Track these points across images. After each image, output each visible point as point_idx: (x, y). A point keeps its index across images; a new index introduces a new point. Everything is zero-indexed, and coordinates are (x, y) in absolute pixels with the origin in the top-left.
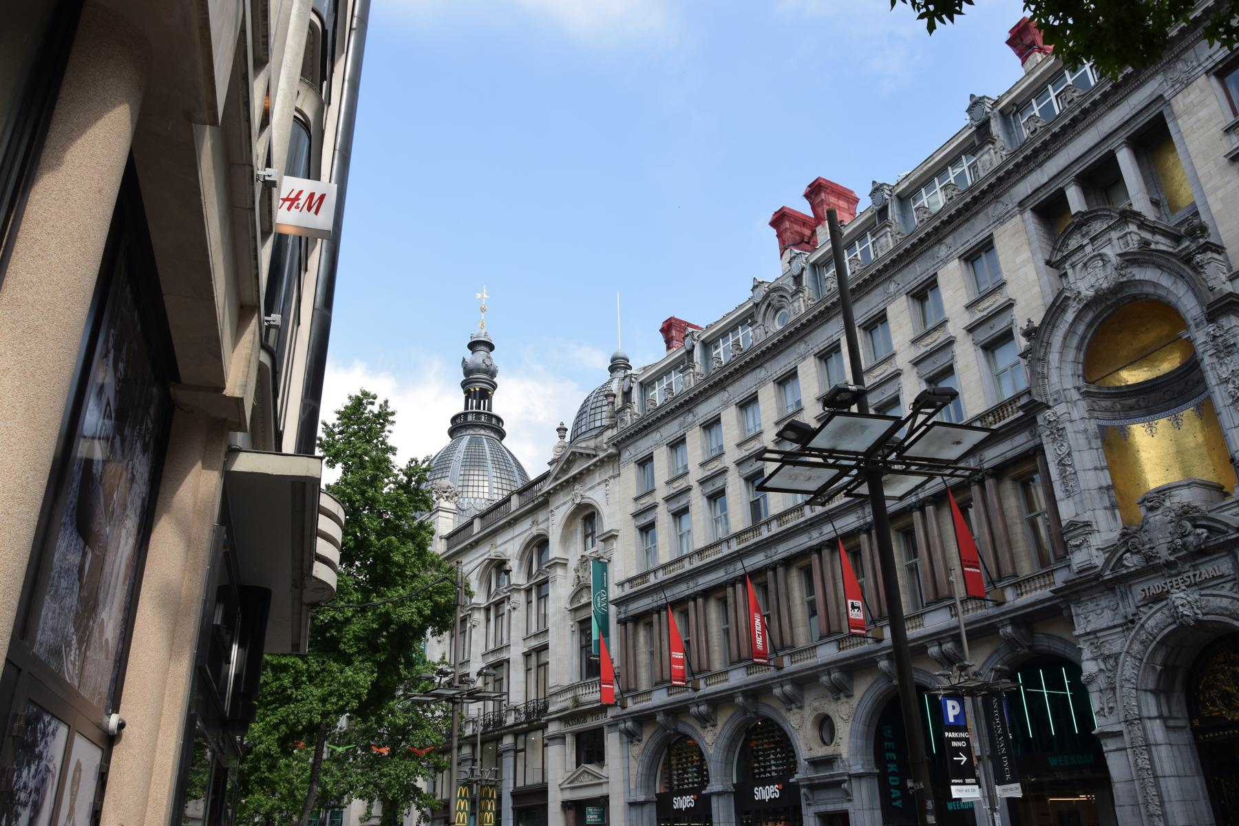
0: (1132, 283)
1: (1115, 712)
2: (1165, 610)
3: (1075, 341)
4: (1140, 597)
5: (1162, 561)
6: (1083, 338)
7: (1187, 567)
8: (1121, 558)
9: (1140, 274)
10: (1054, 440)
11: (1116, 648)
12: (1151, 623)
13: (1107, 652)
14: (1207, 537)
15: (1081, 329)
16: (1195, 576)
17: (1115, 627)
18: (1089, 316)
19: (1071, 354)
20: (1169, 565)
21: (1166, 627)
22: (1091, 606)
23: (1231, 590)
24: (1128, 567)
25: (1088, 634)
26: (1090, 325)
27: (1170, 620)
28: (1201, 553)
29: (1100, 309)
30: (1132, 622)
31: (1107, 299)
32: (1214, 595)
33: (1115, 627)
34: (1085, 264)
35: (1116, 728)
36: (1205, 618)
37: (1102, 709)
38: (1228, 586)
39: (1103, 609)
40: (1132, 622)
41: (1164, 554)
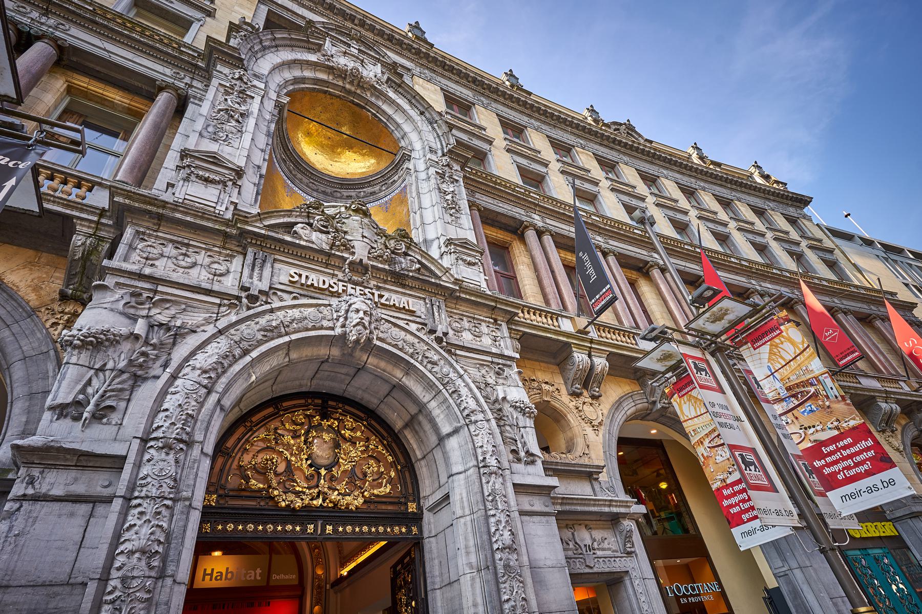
0: (381, 95)
1: (115, 417)
2: (326, 311)
3: (297, 73)
4: (284, 279)
5: (356, 258)
6: (303, 80)
7: (373, 283)
8: (297, 223)
9: (391, 94)
10: (227, 93)
11: (194, 318)
12: (295, 313)
13: (163, 319)
14: (419, 269)
15: (308, 74)
16: (381, 296)
17: (209, 292)
18: (323, 76)
19: (288, 75)
20: (359, 267)
21: (314, 328)
22: (170, 250)
23: (418, 330)
24: (300, 238)
25: (140, 276)
26: (316, 81)
27: (325, 323)
28: (399, 279)
29: (335, 82)
30: (253, 299)
31: (351, 83)
32: (395, 325)
33: (209, 292)
34: (345, 53)
35: (118, 449)
36: (378, 343)
37: (77, 404)
38: (413, 327)
39: (194, 264)
40: (253, 299)
41: (361, 252)
